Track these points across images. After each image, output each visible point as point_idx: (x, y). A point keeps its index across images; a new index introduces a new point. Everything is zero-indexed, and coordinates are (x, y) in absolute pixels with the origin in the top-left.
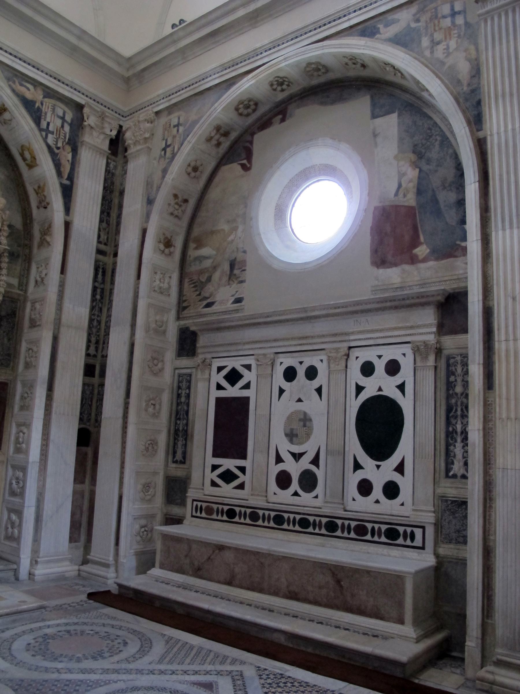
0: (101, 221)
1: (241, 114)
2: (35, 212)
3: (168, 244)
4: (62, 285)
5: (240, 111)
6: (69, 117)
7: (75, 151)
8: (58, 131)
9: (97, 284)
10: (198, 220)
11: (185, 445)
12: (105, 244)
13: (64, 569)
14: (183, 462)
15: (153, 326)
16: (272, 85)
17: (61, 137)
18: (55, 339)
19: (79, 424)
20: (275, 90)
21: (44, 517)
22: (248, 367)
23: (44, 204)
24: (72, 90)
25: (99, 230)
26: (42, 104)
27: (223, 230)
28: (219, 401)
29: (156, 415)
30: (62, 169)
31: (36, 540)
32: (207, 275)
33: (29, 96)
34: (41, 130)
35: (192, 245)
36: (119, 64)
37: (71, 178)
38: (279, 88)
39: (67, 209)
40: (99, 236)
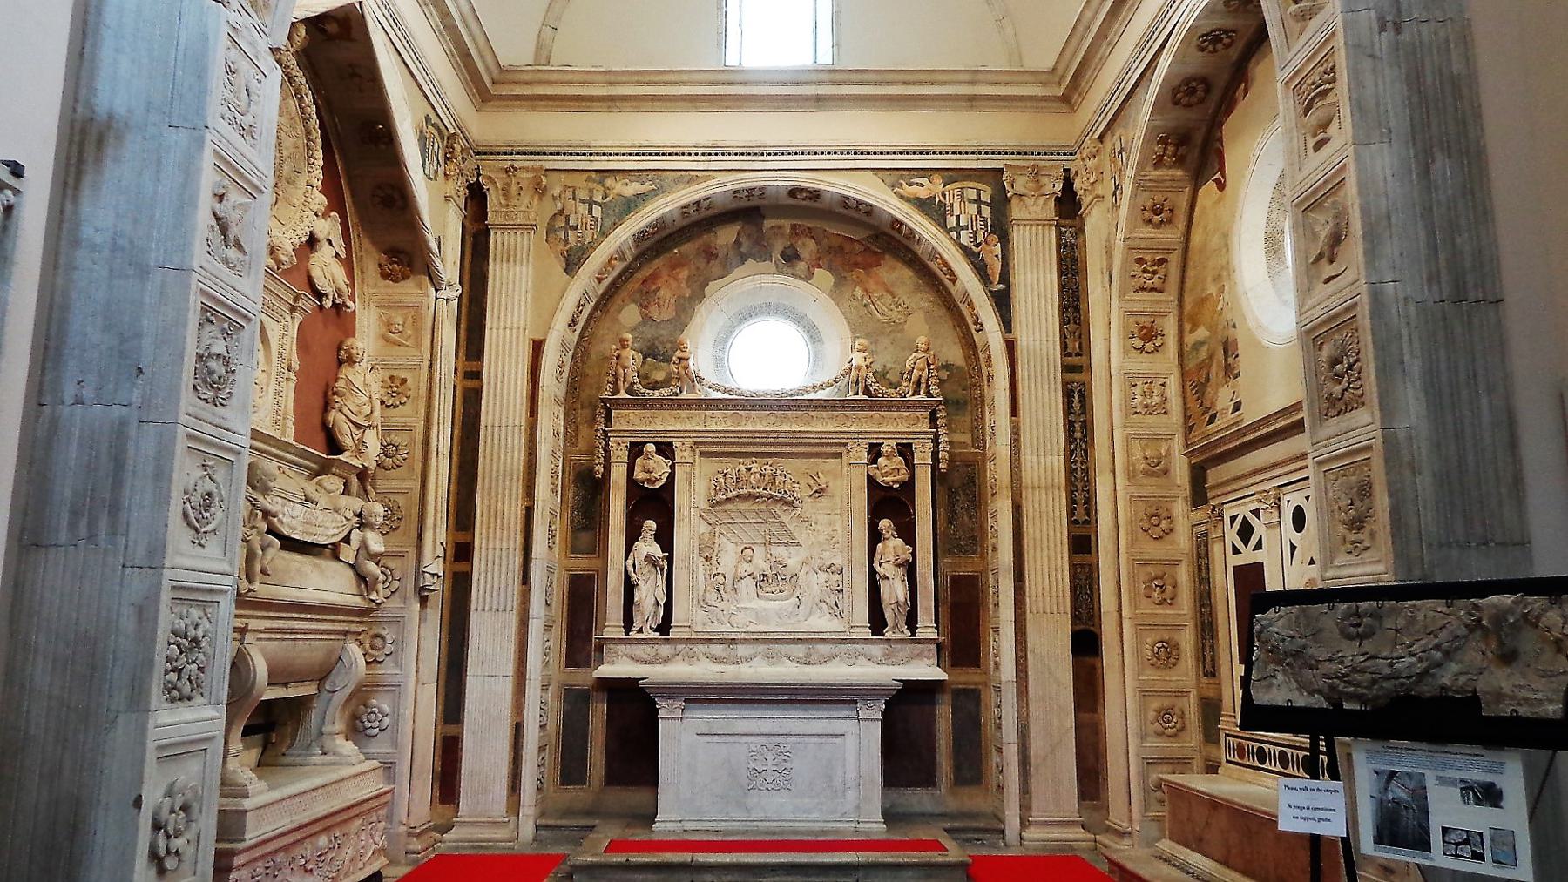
0: (1064, 322)
1: (1188, 106)
2: (976, 336)
3: (1148, 334)
4: (1015, 432)
5: (1185, 101)
6: (985, 197)
7: (1004, 239)
8: (974, 221)
9: (1072, 417)
10: (1189, 284)
11: (1212, 647)
12: (1078, 354)
13: (1071, 836)
14: (1214, 675)
15: (1142, 466)
16: (1202, 49)
17: (979, 227)
18: (1017, 509)
19: (1073, 624)
20: (1215, 51)
21: (1033, 761)
22: (1256, 513)
23: (980, 327)
24: (981, 157)
25: (1063, 336)
26: (944, 196)
27: (1212, 295)
28: (1238, 570)
29: (1169, 601)
30: (989, 272)
31: (1025, 791)
32: (1204, 372)
33: (923, 193)
34: (948, 231)
35: (1187, 326)
36: (1044, 84)
37: (1005, 277)
38: (1219, 46)
39: (1007, 324)
40: (1064, 347)
